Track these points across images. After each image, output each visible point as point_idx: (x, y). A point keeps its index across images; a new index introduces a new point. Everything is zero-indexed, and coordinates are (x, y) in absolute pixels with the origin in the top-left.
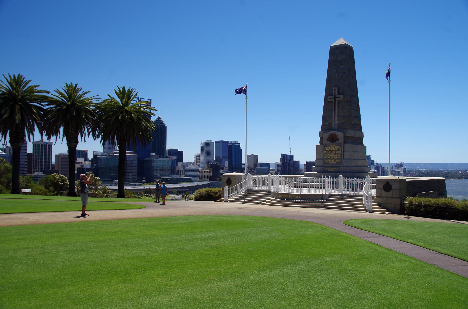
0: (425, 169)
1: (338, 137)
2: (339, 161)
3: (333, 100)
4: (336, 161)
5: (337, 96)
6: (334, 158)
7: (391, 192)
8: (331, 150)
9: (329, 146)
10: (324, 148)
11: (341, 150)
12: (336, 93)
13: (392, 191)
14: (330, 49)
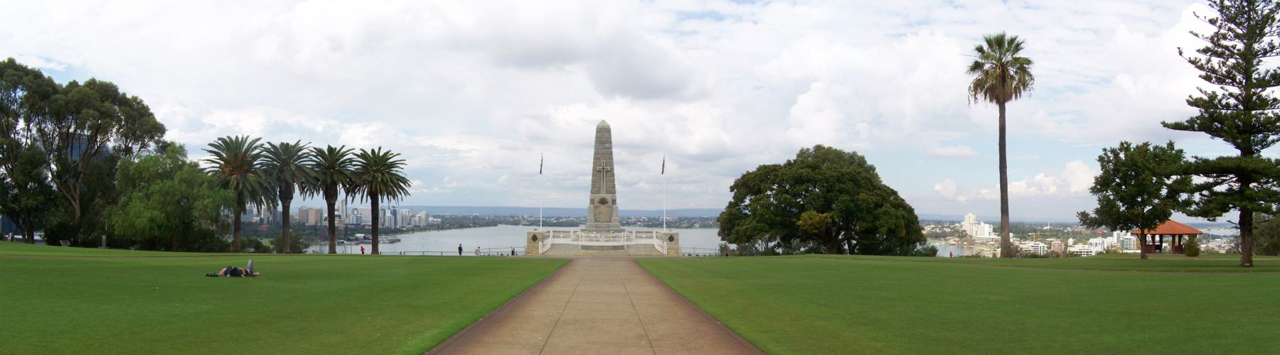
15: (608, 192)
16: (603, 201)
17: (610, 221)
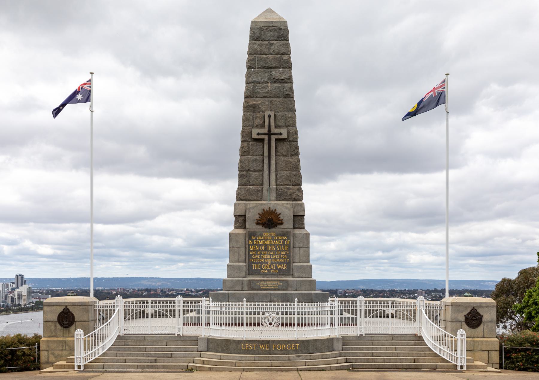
0: (60, 289)
1: (281, 218)
2: (285, 267)
3: (266, 137)
4: (276, 267)
5: (274, 130)
6: (273, 260)
7: (481, 327)
8: (266, 245)
9: (261, 235)
11: (288, 243)
12: (273, 124)
13: (482, 325)
15: (281, 196)
17: (288, 272)
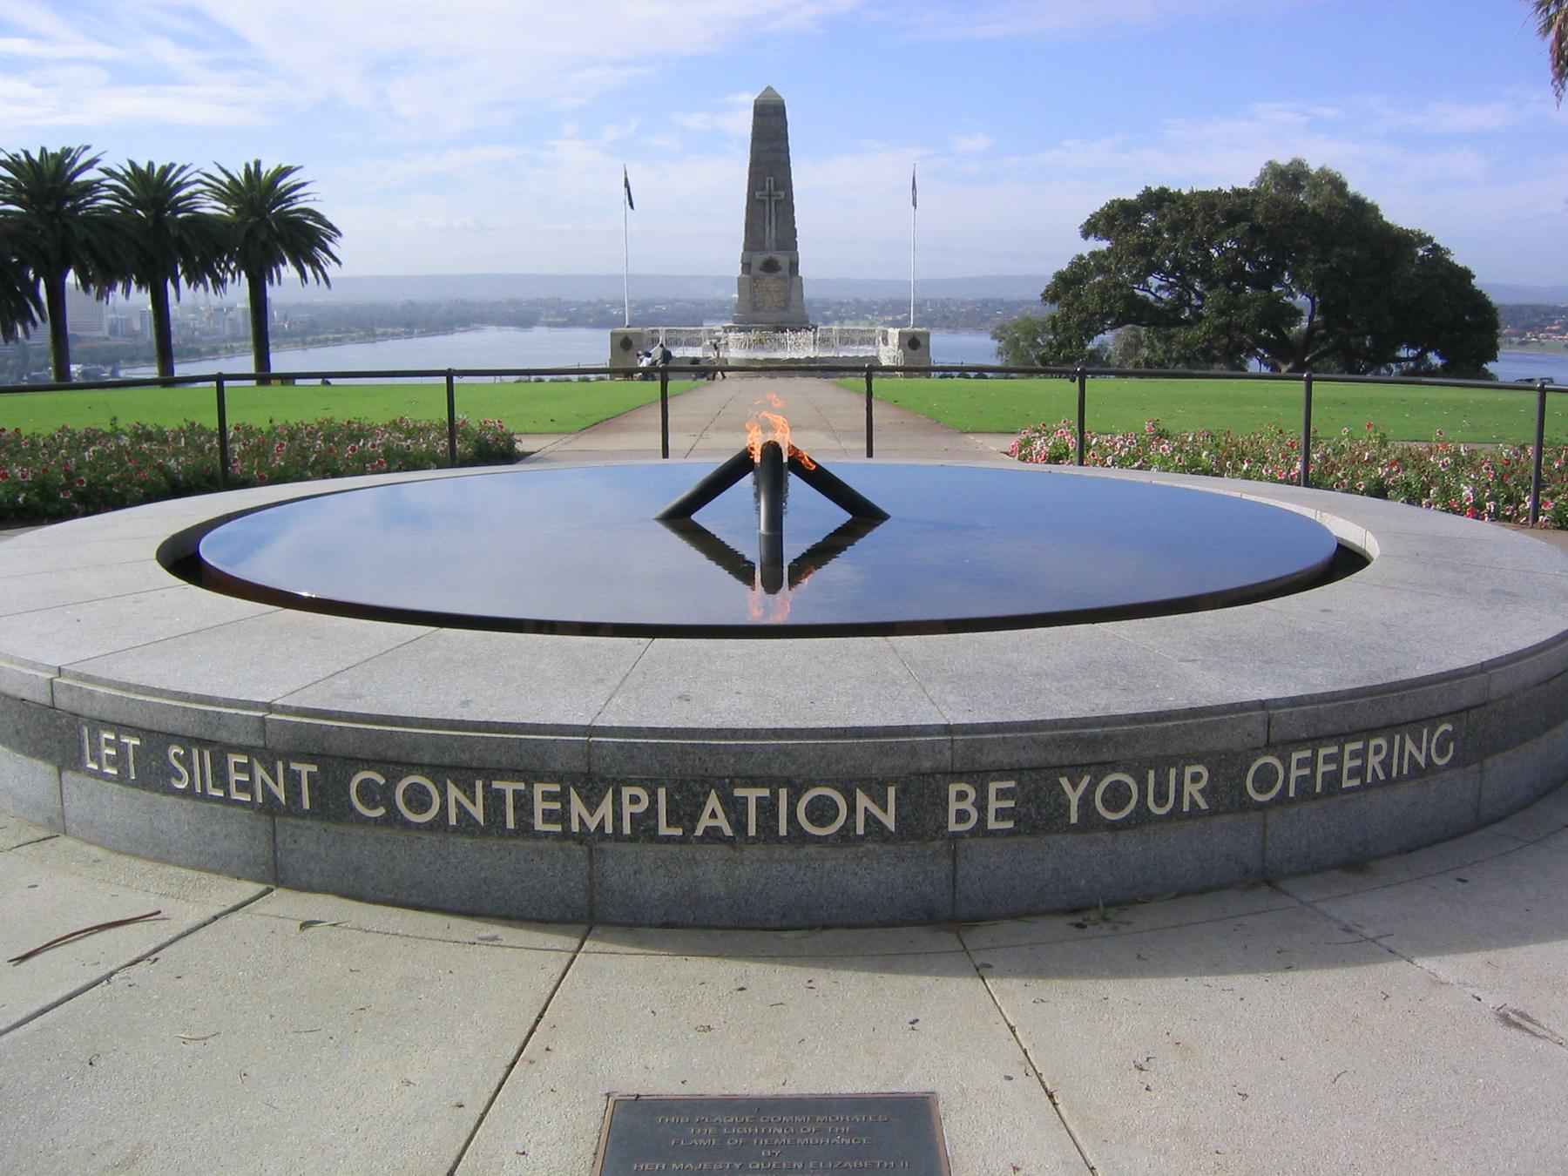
3: (767, 198)
5: (773, 192)
10: (754, 281)
12: (772, 188)
14: (755, 107)
16: (770, 266)
